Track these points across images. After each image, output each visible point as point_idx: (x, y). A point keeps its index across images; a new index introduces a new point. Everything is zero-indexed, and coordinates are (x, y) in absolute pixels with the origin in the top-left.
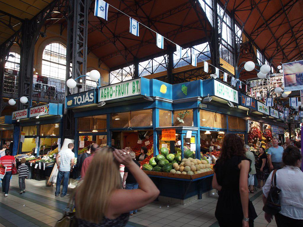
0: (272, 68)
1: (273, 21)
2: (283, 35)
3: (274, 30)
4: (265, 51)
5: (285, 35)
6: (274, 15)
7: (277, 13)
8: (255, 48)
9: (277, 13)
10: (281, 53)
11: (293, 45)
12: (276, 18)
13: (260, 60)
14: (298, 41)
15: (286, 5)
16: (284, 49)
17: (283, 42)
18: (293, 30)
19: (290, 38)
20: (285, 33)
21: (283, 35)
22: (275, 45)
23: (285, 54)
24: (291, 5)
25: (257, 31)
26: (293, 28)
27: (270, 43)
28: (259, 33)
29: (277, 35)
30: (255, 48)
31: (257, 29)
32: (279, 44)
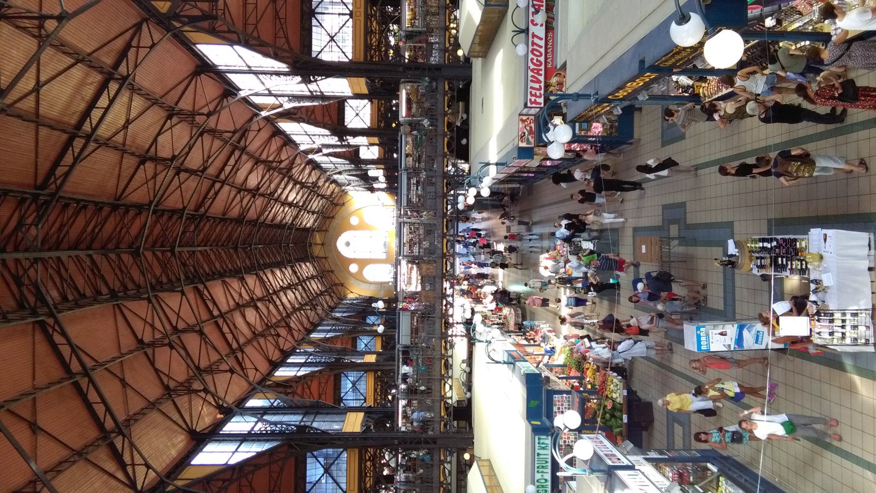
0: (252, 403)
1: (108, 409)
2: (157, 371)
3: (136, 404)
4: (198, 430)
5: (157, 366)
6: (89, 406)
7: (84, 397)
8: (188, 474)
9: (84, 397)
10: (208, 378)
11: (192, 341)
12: (104, 401)
13: (234, 453)
14: (181, 325)
15: (66, 366)
16: (198, 368)
17: (179, 372)
18: (147, 339)
19: (174, 351)
20: (152, 363)
21: (157, 371)
22: (182, 401)
23: (212, 360)
24: (73, 351)
25: (130, 470)
26: (140, 342)
27: (176, 417)
28: (138, 459)
29: (153, 391)
30: (188, 474)
31: (123, 466)
32: (181, 384)
